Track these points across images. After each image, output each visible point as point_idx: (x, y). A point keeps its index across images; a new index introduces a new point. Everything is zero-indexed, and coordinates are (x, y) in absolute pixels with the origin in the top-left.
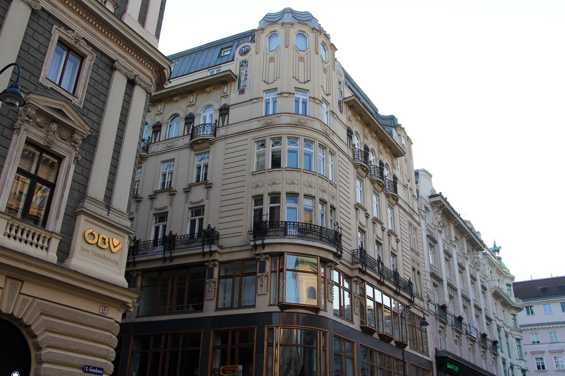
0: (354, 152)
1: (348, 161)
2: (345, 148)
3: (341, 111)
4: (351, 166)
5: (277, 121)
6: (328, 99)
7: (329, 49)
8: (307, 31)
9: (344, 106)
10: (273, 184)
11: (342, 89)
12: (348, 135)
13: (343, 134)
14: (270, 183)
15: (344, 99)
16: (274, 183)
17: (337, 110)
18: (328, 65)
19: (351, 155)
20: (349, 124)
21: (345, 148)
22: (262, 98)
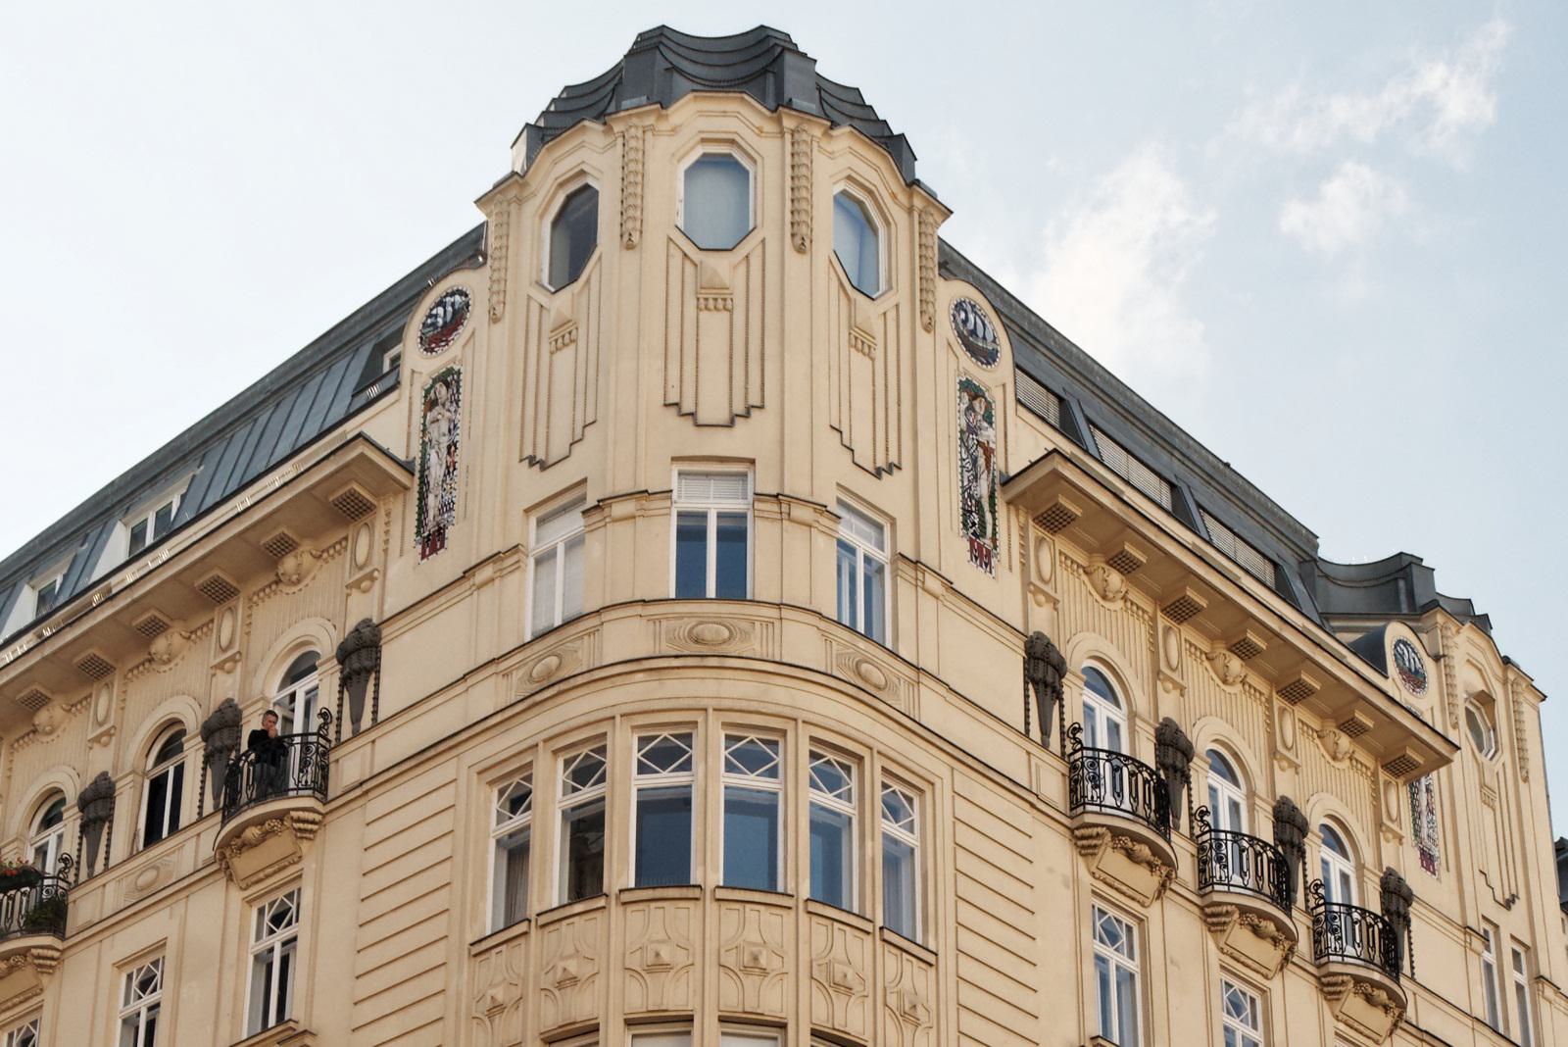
0: (1073, 767)
1: (1024, 818)
2: (1008, 755)
3: (983, 556)
4: (1053, 848)
5: (582, 654)
6: (890, 494)
7: (898, 215)
8: (749, 138)
9: (1008, 527)
10: (560, 985)
11: (988, 434)
12: (1030, 678)
13: (1003, 679)
14: (547, 982)
15: (1007, 481)
16: (569, 982)
17: (952, 552)
18: (886, 304)
19: (1052, 785)
20: (1041, 621)
21: (1008, 755)
22: (515, 549)
